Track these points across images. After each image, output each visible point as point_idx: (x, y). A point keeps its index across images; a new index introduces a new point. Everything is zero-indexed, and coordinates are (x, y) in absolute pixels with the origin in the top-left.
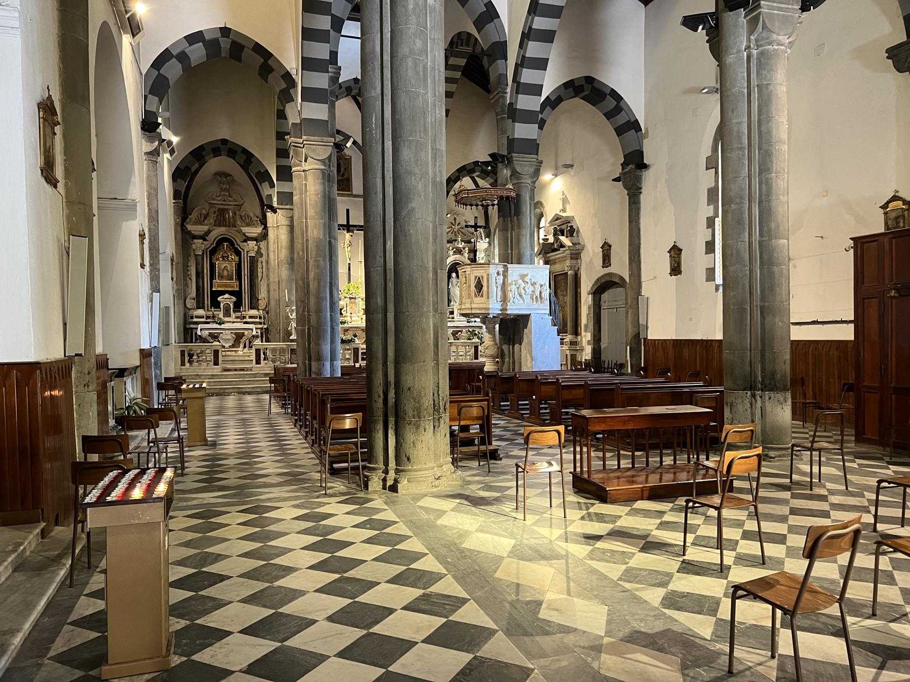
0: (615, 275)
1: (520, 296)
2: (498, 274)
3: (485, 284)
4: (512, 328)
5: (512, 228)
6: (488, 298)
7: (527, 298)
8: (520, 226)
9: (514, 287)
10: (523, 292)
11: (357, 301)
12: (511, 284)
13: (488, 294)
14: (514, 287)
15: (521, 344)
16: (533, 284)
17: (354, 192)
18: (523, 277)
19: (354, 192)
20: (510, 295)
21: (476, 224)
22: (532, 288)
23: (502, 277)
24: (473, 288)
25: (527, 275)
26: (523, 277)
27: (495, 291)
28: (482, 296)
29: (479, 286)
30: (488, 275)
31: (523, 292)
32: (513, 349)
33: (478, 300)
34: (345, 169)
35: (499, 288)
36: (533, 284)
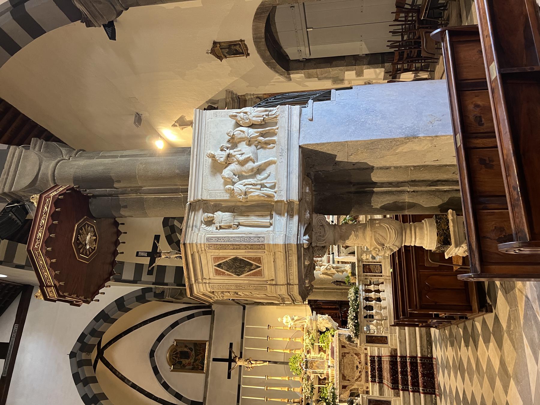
0: (255, 29)
1: (259, 170)
2: (209, 222)
3: (231, 254)
4: (334, 187)
5: (137, 190)
6: (261, 247)
7: (264, 156)
8: (130, 177)
10: (250, 165)
11: (309, 359)
13: (252, 247)
14: (239, 187)
15: (372, 168)
16: (234, 142)
17: (207, 338)
18: (217, 167)
19: (207, 338)
20: (256, 194)
21: (149, 254)
22: (243, 147)
24: (243, 279)
25: (213, 157)
27: (248, 229)
28: (259, 260)
29: (238, 266)
30: (210, 246)
31: (250, 165)
32: (382, 185)
33: (268, 271)
34: (186, 346)
35: (242, 220)
36: (234, 142)
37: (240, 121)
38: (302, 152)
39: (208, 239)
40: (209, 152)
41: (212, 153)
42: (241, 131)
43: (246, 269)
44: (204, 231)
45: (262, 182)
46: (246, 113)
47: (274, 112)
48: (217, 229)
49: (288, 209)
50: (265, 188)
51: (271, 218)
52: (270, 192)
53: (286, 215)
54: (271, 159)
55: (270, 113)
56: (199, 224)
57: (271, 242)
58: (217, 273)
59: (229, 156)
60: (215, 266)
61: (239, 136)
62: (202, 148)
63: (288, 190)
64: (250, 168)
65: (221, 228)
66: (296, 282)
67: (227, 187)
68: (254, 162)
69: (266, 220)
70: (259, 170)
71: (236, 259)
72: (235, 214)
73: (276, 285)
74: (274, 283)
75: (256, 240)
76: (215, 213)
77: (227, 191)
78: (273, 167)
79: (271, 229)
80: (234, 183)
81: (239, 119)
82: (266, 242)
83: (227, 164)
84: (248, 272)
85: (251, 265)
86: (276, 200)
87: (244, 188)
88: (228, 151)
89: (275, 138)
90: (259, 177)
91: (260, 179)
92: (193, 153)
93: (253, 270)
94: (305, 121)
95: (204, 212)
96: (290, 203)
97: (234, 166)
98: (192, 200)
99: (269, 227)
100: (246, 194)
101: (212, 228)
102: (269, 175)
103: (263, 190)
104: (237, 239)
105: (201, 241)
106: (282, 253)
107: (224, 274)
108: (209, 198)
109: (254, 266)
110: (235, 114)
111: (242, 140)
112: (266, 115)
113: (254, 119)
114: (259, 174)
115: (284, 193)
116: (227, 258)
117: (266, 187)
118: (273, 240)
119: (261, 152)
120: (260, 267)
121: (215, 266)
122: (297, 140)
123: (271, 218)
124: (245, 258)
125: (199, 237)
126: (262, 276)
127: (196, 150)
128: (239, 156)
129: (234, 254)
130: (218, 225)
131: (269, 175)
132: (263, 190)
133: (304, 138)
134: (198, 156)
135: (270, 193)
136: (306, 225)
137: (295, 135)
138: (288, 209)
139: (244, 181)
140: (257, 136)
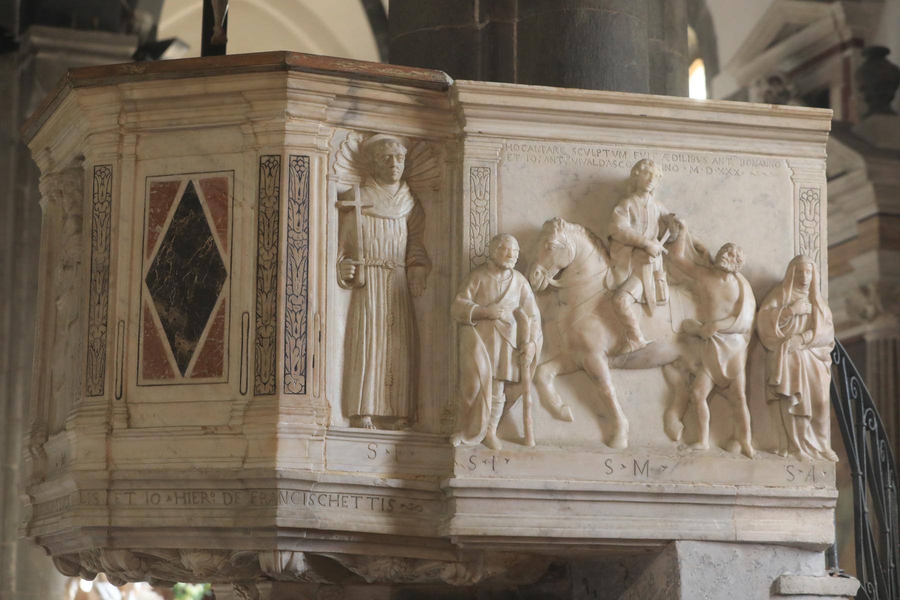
1: (580, 374)
2: (370, 165)
3: (240, 255)
6: (266, 384)
7: (638, 397)
9: (513, 290)
10: (600, 339)
12: (490, 262)
13: (266, 342)
14: (513, 290)
23: (399, 203)
24: (130, 293)
25: (635, 185)
26: (598, 203)
28: (211, 366)
29: (188, 274)
31: (600, 339)
35: (378, 301)
37: (779, 297)
38: (649, 550)
39: (301, 161)
40: (657, 170)
41: (654, 184)
42: (739, 303)
43: (175, 313)
44: (335, 145)
45: (531, 387)
46: (811, 325)
47: (813, 440)
48: (341, 196)
49: (421, 491)
50: (502, 399)
51: (381, 422)
52: (490, 419)
53: (393, 483)
54: (624, 421)
55: (807, 423)
56: (364, 121)
57: (284, 422)
58: (161, 193)
59: (640, 251)
60: (190, 186)
61: (717, 294)
62: (673, 140)
63: (493, 493)
64: (589, 337)
65: (346, 212)
66: (123, 520)
67: (514, 247)
68: (612, 354)
69: (374, 403)
70: (580, 374)
71: (216, 272)
72: (401, 271)
73: (110, 432)
74: (118, 424)
75: (296, 360)
76: (405, 190)
77: (497, 240)
78: (591, 430)
79: (338, 420)
80: (524, 267)
81: (790, 294)
82: (285, 400)
83: (608, 242)
84: (164, 321)
85: (193, 335)
86: (457, 443)
87: (507, 314)
88: (658, 247)
89: (707, 442)
90: (550, 374)
91: (543, 377)
92: (654, 104)
93: (171, 339)
94: (774, 565)
95: (411, 142)
96: (444, 498)
97: (595, 268)
98: (464, 97)
99: (345, 414)
100: (485, 319)
101: (343, 175)
102: (555, 414)
103: (495, 392)
104: (298, 283)
105: (295, 132)
106: (236, 465)
107: (157, 218)
108: (469, 163)
109: (185, 345)
110: (808, 278)
111: (704, 303)
112: (800, 407)
113: (785, 360)
114: (564, 375)
115: (481, 476)
116: (223, 236)
117: (508, 404)
118: (296, 431)
119: (652, 383)
120: (183, 368)
121: (190, 186)
122: (696, 534)
123: (381, 422)
124: (222, 312)
125: (312, 123)
126: (146, 376)
127: (666, 113)
128: (637, 291)
129: (236, 267)
130: (358, 203)
131: (555, 414)
132: (495, 392)
133: (705, 560)
134: (639, 123)
135: (485, 419)
136: (344, 562)
137: (717, 524)
138: (421, 491)
139: (536, 311)
140: (716, 369)
